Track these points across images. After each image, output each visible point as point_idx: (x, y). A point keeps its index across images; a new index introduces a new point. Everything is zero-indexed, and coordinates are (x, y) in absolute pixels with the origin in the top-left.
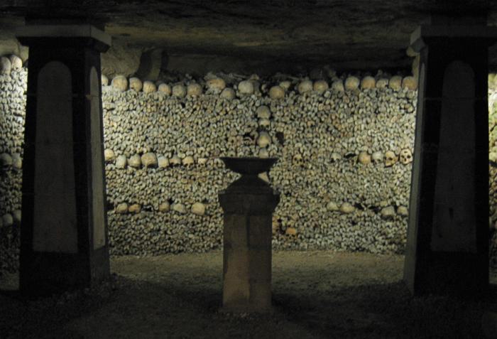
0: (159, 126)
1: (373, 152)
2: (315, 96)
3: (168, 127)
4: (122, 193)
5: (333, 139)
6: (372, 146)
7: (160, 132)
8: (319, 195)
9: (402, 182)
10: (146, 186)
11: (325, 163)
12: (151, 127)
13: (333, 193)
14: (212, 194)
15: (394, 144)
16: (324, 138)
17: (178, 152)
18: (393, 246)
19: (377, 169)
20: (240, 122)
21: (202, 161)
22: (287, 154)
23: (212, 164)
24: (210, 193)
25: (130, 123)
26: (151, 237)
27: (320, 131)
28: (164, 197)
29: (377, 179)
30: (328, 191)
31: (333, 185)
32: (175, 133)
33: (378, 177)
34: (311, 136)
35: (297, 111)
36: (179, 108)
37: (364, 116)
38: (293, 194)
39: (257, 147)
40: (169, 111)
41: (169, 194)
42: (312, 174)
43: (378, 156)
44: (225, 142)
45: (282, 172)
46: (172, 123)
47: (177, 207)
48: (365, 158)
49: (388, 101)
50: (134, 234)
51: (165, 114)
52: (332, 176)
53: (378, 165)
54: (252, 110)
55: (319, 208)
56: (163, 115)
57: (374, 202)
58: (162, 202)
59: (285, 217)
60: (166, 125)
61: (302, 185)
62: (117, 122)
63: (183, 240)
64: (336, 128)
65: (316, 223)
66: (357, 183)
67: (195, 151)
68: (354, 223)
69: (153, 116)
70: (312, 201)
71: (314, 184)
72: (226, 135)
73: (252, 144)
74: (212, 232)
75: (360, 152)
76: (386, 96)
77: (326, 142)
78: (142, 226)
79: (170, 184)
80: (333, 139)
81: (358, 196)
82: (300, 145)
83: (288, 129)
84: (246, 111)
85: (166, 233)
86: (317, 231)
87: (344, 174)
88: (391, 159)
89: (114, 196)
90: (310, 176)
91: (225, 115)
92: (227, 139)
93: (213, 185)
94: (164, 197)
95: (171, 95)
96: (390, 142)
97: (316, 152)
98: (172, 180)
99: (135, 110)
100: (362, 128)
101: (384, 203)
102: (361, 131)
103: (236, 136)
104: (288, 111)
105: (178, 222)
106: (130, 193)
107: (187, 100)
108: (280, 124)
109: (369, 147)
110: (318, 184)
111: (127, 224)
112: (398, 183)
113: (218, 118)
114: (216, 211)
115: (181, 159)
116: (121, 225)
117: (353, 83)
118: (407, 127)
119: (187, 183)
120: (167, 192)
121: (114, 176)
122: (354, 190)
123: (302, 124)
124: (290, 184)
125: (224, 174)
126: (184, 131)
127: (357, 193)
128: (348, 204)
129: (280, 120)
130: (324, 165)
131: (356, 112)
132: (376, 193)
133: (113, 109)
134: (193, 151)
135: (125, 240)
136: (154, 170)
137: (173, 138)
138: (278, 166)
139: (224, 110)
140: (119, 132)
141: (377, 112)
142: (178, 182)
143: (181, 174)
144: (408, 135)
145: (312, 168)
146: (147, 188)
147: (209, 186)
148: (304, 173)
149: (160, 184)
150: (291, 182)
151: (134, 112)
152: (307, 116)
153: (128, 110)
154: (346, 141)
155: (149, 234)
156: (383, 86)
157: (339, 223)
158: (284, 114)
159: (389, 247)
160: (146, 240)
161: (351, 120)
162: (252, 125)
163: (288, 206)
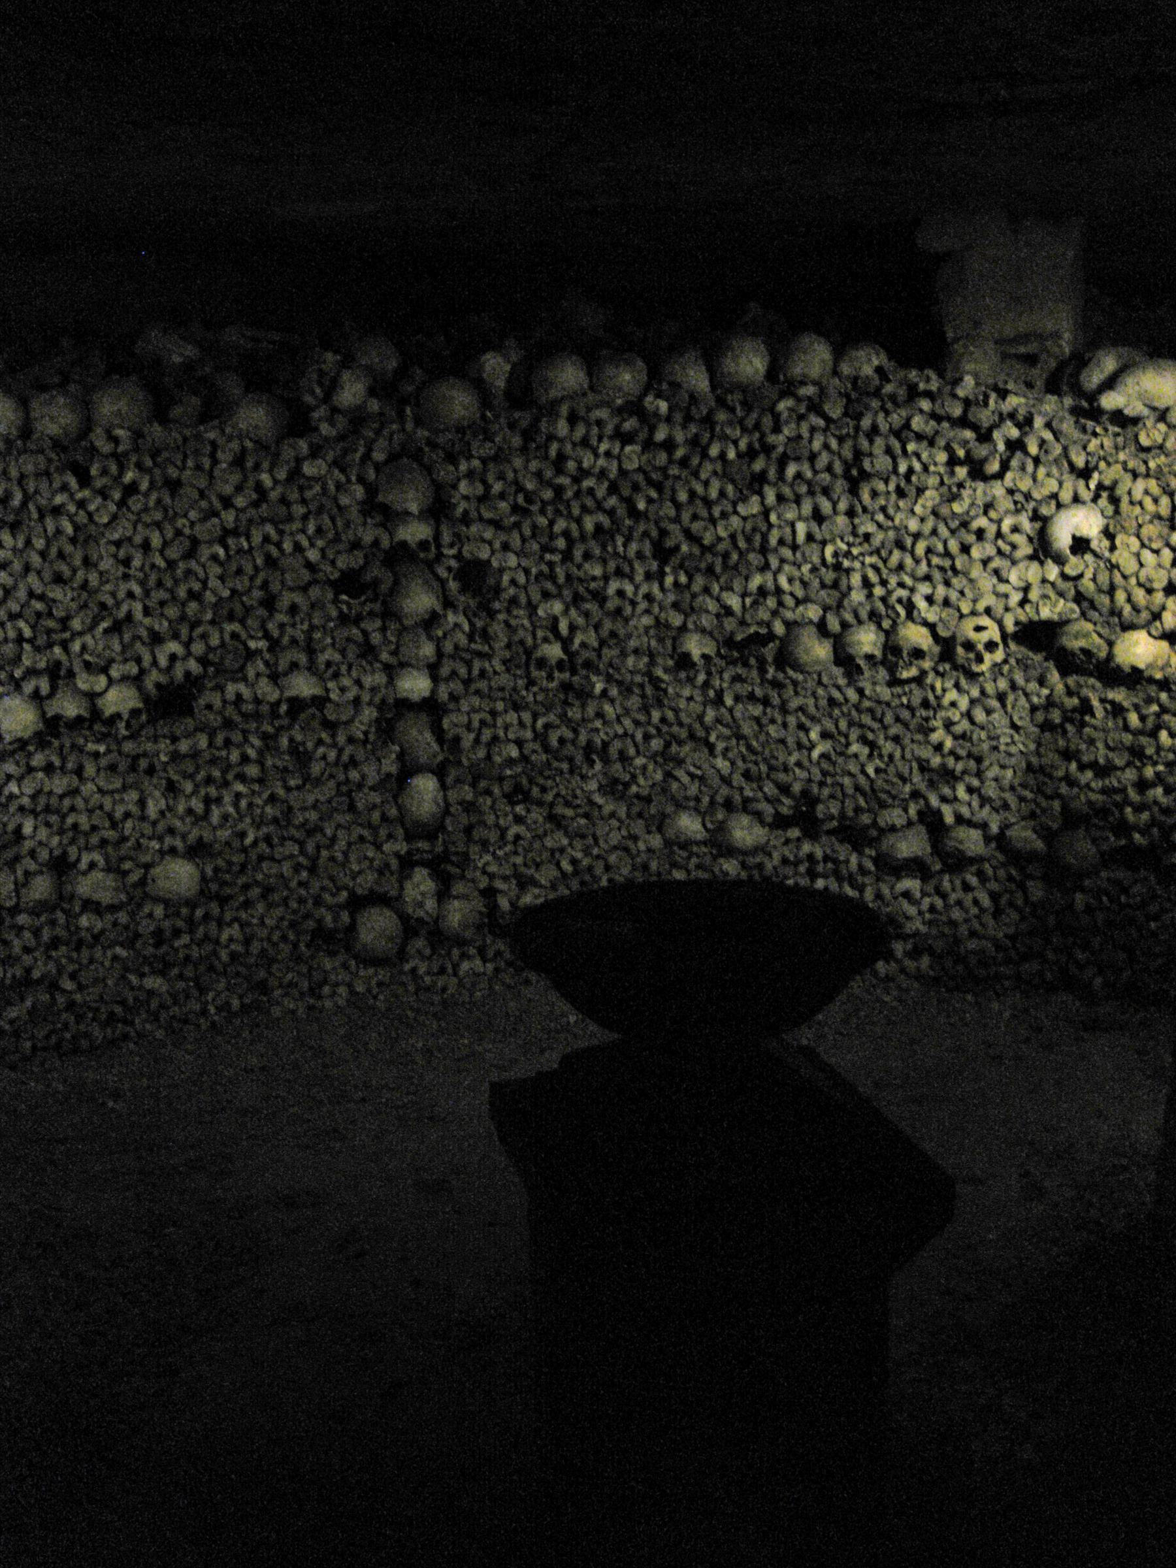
1: (845, 625)
3: (27, 568)
6: (840, 605)
8: (634, 789)
9: (963, 736)
11: (659, 672)
13: (686, 779)
14: (225, 817)
15: (930, 599)
16: (648, 576)
17: (77, 667)
18: (925, 961)
19: (861, 692)
20: (319, 531)
22: (508, 646)
23: (217, 703)
24: (215, 818)
27: (634, 547)
28: (32, 854)
29: (861, 726)
32: (56, 593)
33: (866, 719)
35: (539, 475)
36: (64, 488)
37: (803, 489)
38: (535, 791)
40: (24, 504)
41: (55, 840)
43: (867, 640)
44: (262, 612)
46: (43, 554)
49: (902, 432)
52: (686, 720)
53: (867, 674)
54: (361, 480)
55: (635, 838)
57: (851, 814)
58: (27, 873)
59: (505, 878)
60: (17, 566)
61: (571, 760)
63: (123, 1003)
64: (689, 535)
66: (783, 741)
71: (613, 751)
72: (265, 585)
73: (371, 614)
74: (234, 956)
75: (788, 624)
79: (54, 801)
80: (683, 579)
81: (785, 789)
82: (557, 607)
84: (339, 487)
85: (54, 987)
88: (918, 653)
90: (598, 724)
91: (256, 504)
92: (269, 603)
93: (226, 784)
94: (32, 854)
95: (26, 432)
96: (912, 590)
97: (622, 632)
98: (59, 784)
102: (795, 547)
103: (304, 589)
104: (501, 477)
105: (96, 938)
107: (93, 450)
110: (632, 751)
112: (949, 743)
113: (229, 517)
114: (241, 881)
118: (980, 534)
120: (43, 833)
123: (561, 525)
124: (524, 758)
125: (265, 737)
127: (782, 777)
128: (745, 820)
129: (474, 514)
130: (655, 682)
131: (772, 474)
132: (862, 780)
134: (138, 660)
137: (50, 614)
138: (478, 692)
139: (251, 483)
141: (856, 476)
142: (88, 788)
143: (96, 755)
144: (985, 562)
145: (604, 693)
147: (213, 791)
148: (574, 713)
150: (529, 746)
152: (577, 494)
154: (737, 585)
156: (868, 370)
158: (487, 487)
159: (909, 964)
161: (753, 507)
162: (368, 538)
163: (518, 837)
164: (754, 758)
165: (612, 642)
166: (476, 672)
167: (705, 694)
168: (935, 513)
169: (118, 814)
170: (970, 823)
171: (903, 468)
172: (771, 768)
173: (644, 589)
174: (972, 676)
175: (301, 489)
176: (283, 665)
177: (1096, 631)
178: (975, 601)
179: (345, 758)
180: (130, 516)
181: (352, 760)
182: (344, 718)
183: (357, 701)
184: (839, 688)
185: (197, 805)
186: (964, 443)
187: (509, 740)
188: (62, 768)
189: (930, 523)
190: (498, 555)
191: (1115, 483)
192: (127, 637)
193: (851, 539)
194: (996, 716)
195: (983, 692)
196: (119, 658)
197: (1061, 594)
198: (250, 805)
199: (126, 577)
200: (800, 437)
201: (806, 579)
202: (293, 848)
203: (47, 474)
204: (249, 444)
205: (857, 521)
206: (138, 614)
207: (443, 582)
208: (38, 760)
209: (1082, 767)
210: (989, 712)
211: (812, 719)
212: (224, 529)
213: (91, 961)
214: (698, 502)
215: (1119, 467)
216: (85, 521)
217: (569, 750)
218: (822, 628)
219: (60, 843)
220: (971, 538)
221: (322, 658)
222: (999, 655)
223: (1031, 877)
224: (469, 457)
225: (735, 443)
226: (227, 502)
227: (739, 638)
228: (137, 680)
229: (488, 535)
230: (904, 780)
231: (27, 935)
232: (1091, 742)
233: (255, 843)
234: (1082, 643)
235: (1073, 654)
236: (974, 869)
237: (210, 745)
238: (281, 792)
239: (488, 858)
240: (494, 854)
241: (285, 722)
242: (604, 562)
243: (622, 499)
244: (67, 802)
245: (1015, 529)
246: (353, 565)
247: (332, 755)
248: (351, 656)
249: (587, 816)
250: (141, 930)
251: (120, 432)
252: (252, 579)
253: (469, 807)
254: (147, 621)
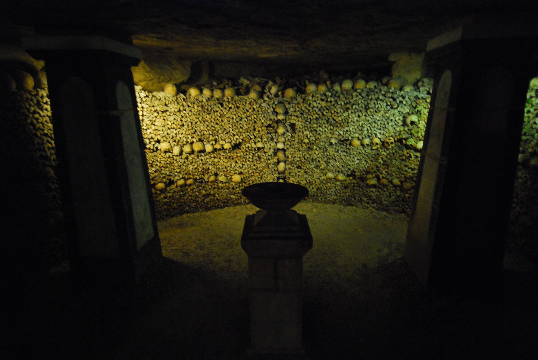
0: (204, 122)
1: (363, 138)
2: (318, 95)
3: (211, 122)
4: (180, 172)
5: (332, 128)
6: (362, 134)
7: (206, 126)
10: (198, 166)
11: (326, 146)
12: (199, 123)
14: (246, 168)
15: (380, 133)
16: (325, 127)
19: (365, 151)
20: (264, 117)
24: (244, 168)
25: (181, 121)
26: (204, 200)
29: (365, 158)
30: (328, 165)
31: (331, 161)
32: (216, 126)
33: (366, 157)
34: (315, 125)
35: (306, 107)
36: (219, 107)
37: (356, 111)
38: (302, 167)
39: (277, 135)
40: (211, 110)
42: (317, 153)
43: (367, 141)
45: (295, 152)
46: (214, 119)
47: (221, 178)
48: (357, 143)
50: (191, 199)
51: (209, 112)
52: (331, 154)
54: (273, 107)
55: (321, 177)
56: (207, 113)
57: (362, 175)
60: (209, 121)
61: (309, 161)
63: (227, 200)
65: (319, 186)
66: (350, 160)
67: (232, 139)
68: (346, 187)
69: (199, 114)
70: (315, 171)
71: (317, 160)
73: (273, 132)
75: (352, 137)
76: (375, 95)
77: (327, 130)
78: (197, 193)
79: (215, 163)
80: (332, 128)
81: (349, 169)
82: (307, 132)
83: (299, 121)
84: (268, 108)
85: (214, 196)
86: (319, 192)
87: (340, 154)
88: (377, 144)
89: (173, 175)
90: (314, 155)
92: (254, 130)
95: (212, 97)
97: (319, 137)
98: (216, 160)
99: (185, 110)
100: (355, 120)
101: (369, 176)
102: (354, 122)
103: (261, 127)
104: (298, 107)
106: (186, 172)
107: (224, 101)
108: (293, 117)
109: (360, 135)
110: (320, 160)
111: (186, 193)
113: (248, 114)
114: (249, 179)
115: (222, 145)
116: (181, 195)
117: (347, 85)
118: (391, 120)
119: (228, 162)
120: (213, 169)
121: (172, 161)
122: (347, 165)
124: (301, 160)
125: (253, 154)
126: (223, 124)
127: (349, 167)
128: (342, 175)
129: (293, 115)
130: (325, 147)
131: (350, 108)
132: (364, 169)
133: (167, 111)
134: (231, 139)
135: (185, 203)
136: (203, 154)
137: (215, 130)
138: (292, 148)
139: (252, 108)
140: (174, 128)
141: (367, 108)
143: (223, 155)
144: (392, 126)
145: (316, 149)
146: (199, 167)
147: (244, 163)
148: (310, 152)
149: (208, 164)
151: (184, 112)
153: (180, 111)
155: (203, 198)
156: (372, 87)
157: (335, 187)
159: (373, 205)
160: (201, 202)
161: (346, 114)
164: (344, 163)
165: (318, 139)
166: (292, 144)
167: (335, 150)
168: (382, 116)
169: (227, 166)
170: (385, 178)
171: (377, 107)
172: (347, 165)
173: (324, 130)
174: (388, 149)
175: (261, 109)
177: (414, 141)
178: (389, 134)
179: (267, 159)
180: (230, 113)
181: (269, 159)
182: (268, 151)
183: (270, 148)
184: (361, 150)
185: (241, 165)
186: (390, 102)
187: (298, 157)
188: (217, 157)
189: (382, 118)
190: (297, 122)
191: (421, 110)
192: (229, 135)
193: (365, 121)
194: (392, 157)
195: (390, 152)
196: (227, 139)
197: (408, 133)
198: (250, 166)
199: (229, 124)
200: (357, 100)
201: (356, 129)
202: (257, 174)
203: (216, 105)
204: (252, 100)
205: (367, 117)
206: (231, 131)
207: (286, 127)
208: (212, 156)
209: (409, 168)
210: (391, 156)
211: (356, 156)
212: (247, 116)
213: (221, 192)
214: (336, 113)
215: (422, 107)
216: (222, 114)
218: (358, 138)
219: (216, 171)
220: (389, 121)
221: (263, 140)
222: (393, 145)
223: (397, 190)
224: (293, 103)
226: (248, 111)
227: (342, 140)
228: (230, 142)
230: (372, 169)
231: (210, 186)
232: (411, 163)
233: (251, 173)
234: (411, 143)
235: (409, 146)
236: (386, 187)
237: (244, 155)
238: (256, 164)
239: (293, 178)
240: (294, 178)
241: (257, 151)
242: (317, 124)
244: (217, 164)
245: (399, 119)
246: (270, 123)
247: (265, 158)
248: (269, 140)
249: (312, 172)
250: (230, 187)
251: (229, 97)
252: (252, 125)
253: (290, 169)
254: (233, 132)
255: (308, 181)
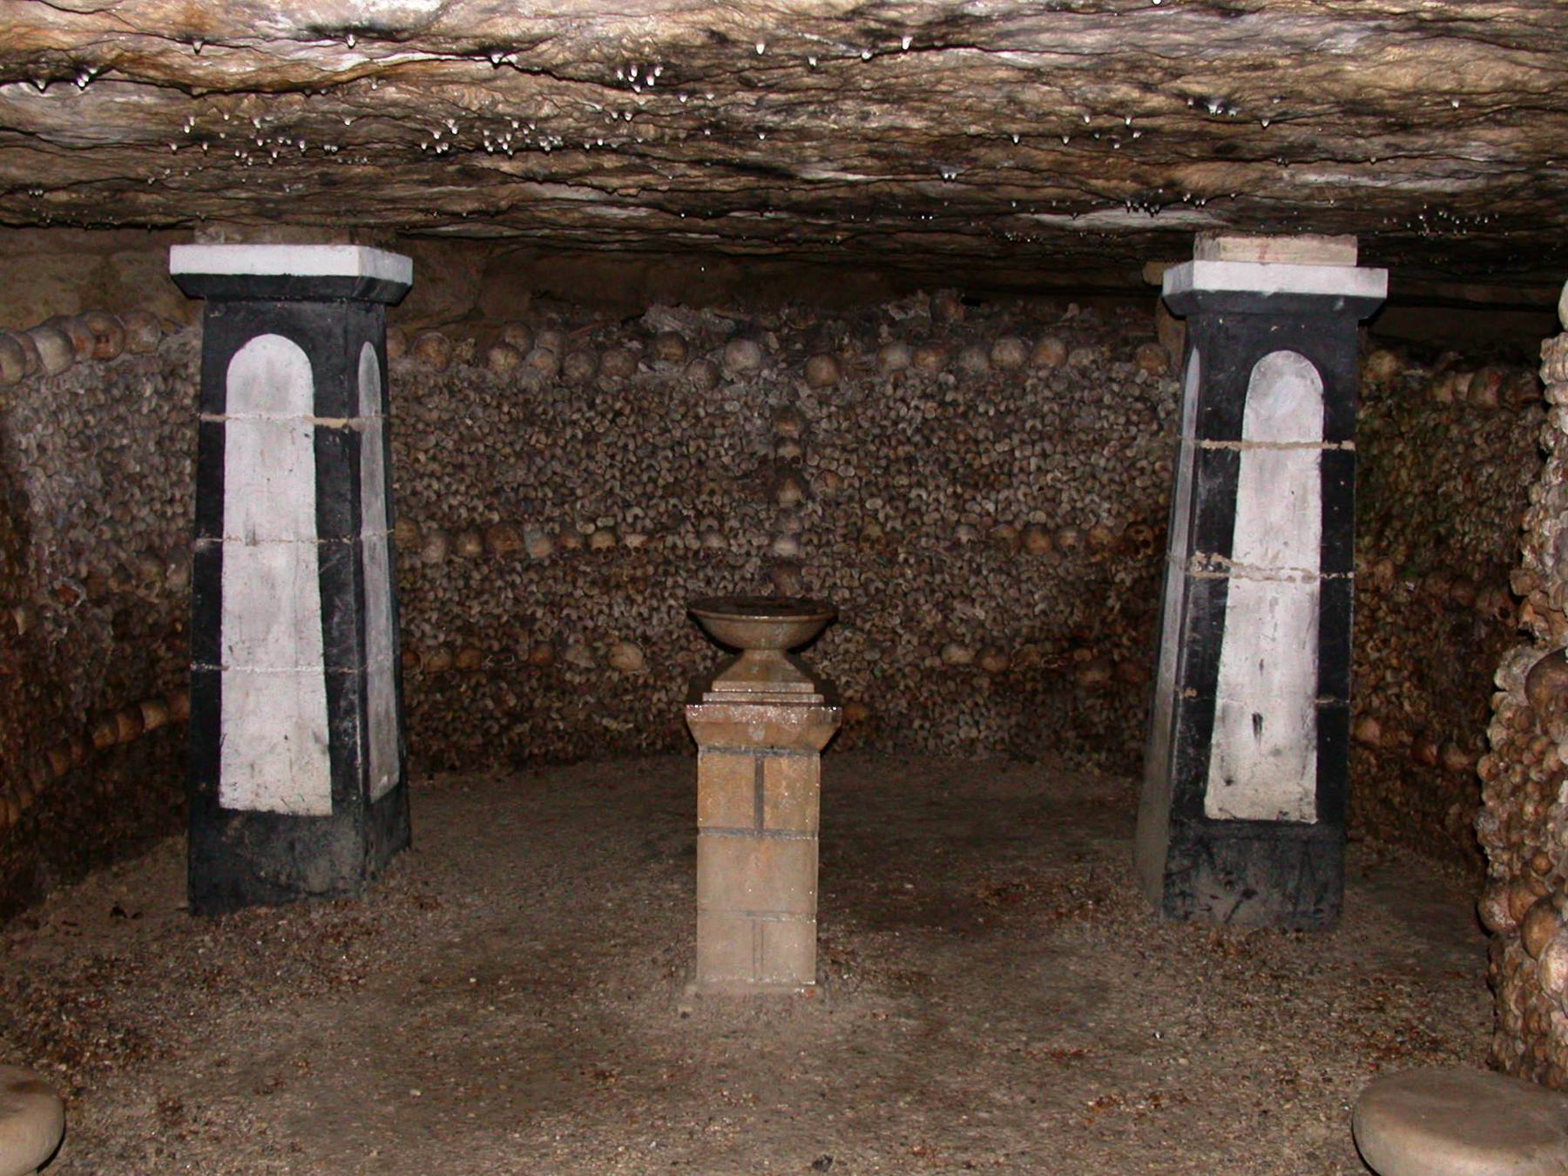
5: (959, 490)
13: (957, 622)
15: (1109, 511)
16: (937, 487)
20: (732, 446)
21: (634, 541)
28: (541, 631)
34: (905, 481)
38: (859, 622)
39: (773, 509)
45: (834, 569)
49: (1098, 402)
62: (426, 452)
66: (1017, 600)
67: (619, 519)
82: (879, 502)
84: (746, 419)
90: (901, 581)
91: (694, 426)
100: (1033, 467)
101: (1083, 654)
113: (677, 434)
118: (1142, 470)
134: (615, 516)
142: (578, 593)
143: (585, 573)
147: (655, 603)
161: (1002, 447)
162: (762, 452)
163: (847, 651)
173: (933, 496)
176: (703, 527)
183: (748, 554)
199: (611, 466)
217: (881, 596)
225: (996, 405)
229: (837, 455)
243: (924, 437)
255: (877, 673)
